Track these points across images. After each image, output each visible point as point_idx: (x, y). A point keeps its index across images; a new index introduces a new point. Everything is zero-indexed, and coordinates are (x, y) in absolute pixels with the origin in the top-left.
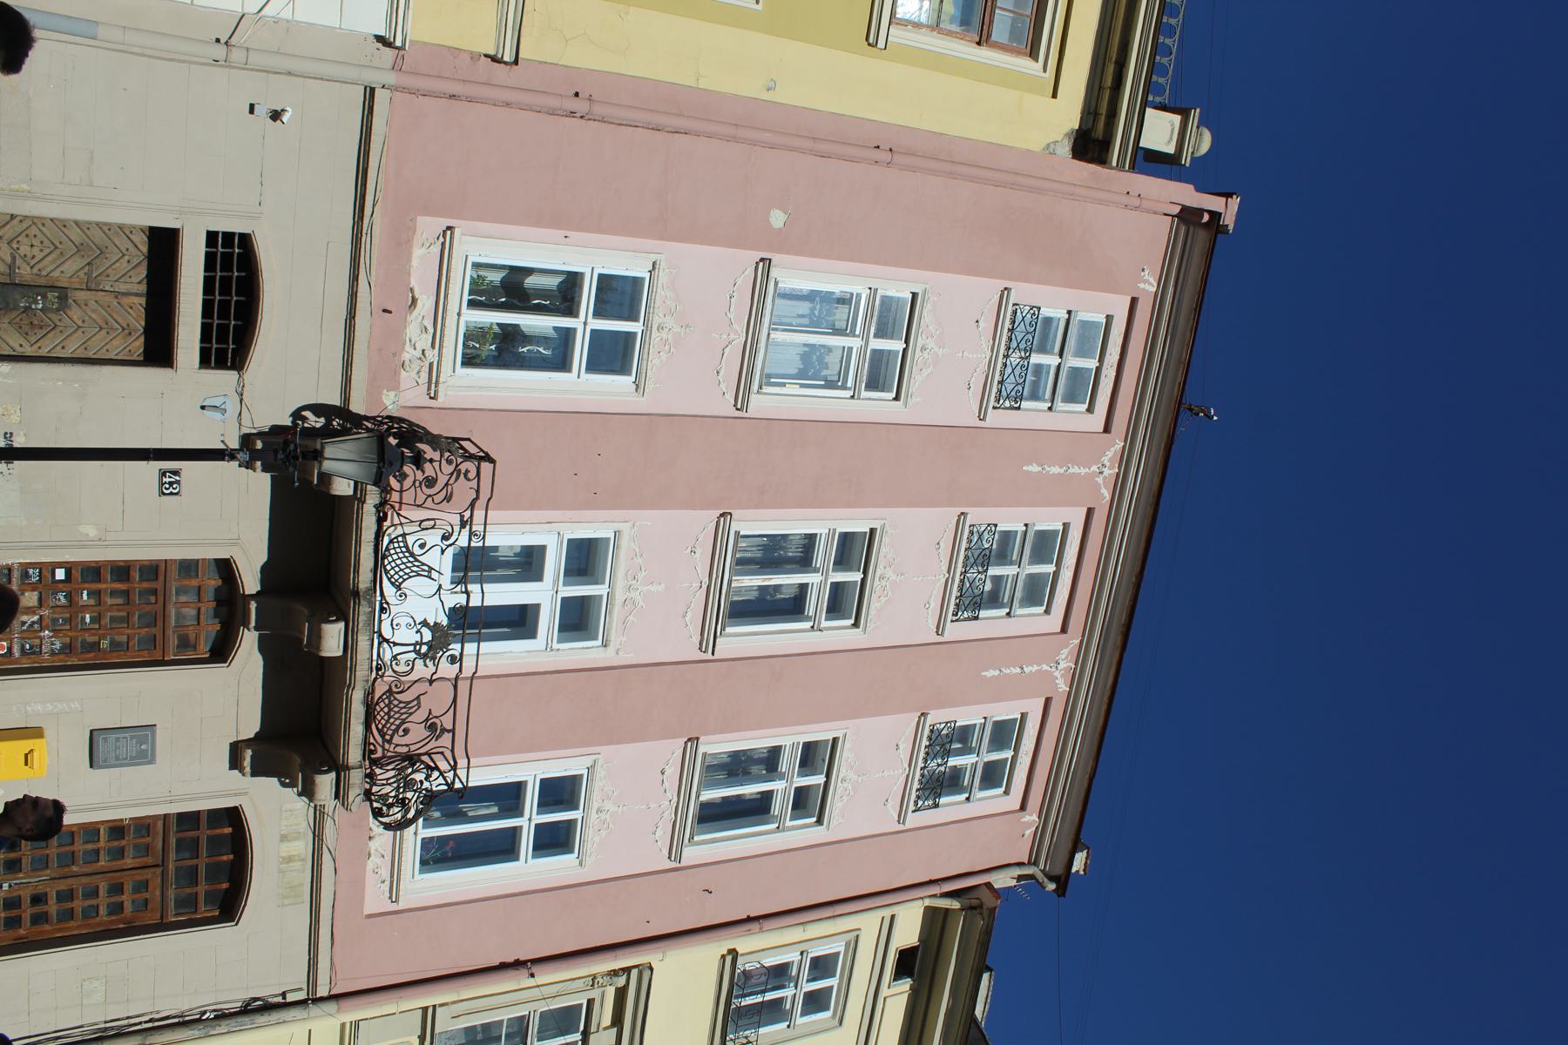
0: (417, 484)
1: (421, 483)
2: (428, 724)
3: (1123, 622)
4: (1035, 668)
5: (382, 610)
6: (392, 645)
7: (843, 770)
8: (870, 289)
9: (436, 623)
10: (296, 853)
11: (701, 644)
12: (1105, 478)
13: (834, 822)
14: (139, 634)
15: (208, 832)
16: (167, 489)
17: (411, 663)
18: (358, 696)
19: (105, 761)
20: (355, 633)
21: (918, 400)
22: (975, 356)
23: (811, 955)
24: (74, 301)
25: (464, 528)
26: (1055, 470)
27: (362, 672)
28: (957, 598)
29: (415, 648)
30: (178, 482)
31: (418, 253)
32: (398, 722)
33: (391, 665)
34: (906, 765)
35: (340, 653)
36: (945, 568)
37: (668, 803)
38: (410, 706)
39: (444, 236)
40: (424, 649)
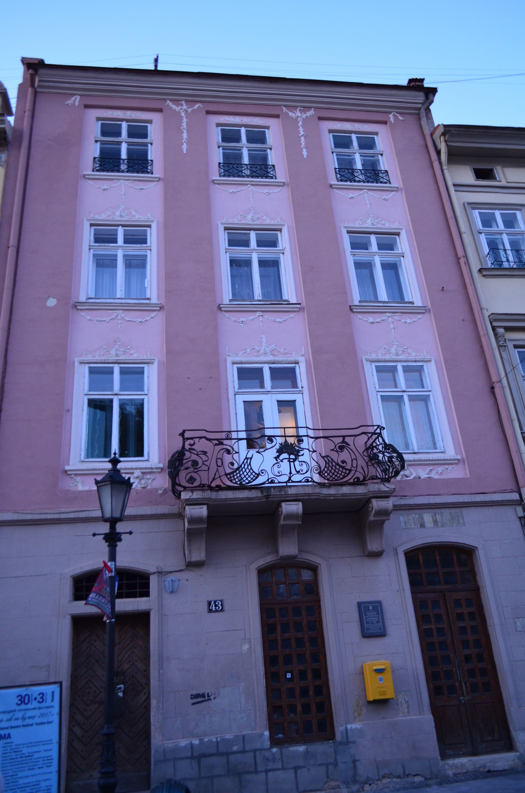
0: (196, 470)
1: (195, 469)
2: (340, 450)
4: (301, 129)
5: (272, 482)
6: (291, 475)
10: (431, 518)
11: (295, 311)
12: (188, 108)
15: (422, 568)
16: (219, 608)
17: (301, 463)
18: (325, 491)
20: (287, 495)
22: (123, 188)
23: (481, 228)
24: (119, 668)
25: (223, 443)
26: (185, 135)
27: (309, 491)
29: (292, 462)
30: (215, 602)
31: (80, 488)
32: (338, 467)
33: (303, 474)
34: (362, 192)
35: (300, 504)
36: (245, 187)
37: (390, 319)
38: (327, 461)
39: (71, 475)
40: (292, 457)
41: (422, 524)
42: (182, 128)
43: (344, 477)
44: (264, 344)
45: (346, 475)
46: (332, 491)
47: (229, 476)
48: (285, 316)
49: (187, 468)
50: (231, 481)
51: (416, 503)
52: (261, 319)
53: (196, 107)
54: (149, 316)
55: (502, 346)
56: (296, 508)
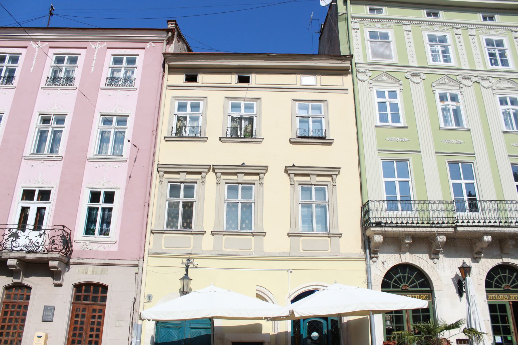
3: (81, 30)
4: (95, 55)
5: (4, 250)
7: (112, 111)
9: (8, 236)
12: (41, 45)
14: (23, 309)
18: (29, 255)
19: (50, 318)
26: (34, 62)
28: (67, 85)
32: (33, 245)
34: (117, 91)
52: (42, 164)
53: (44, 45)
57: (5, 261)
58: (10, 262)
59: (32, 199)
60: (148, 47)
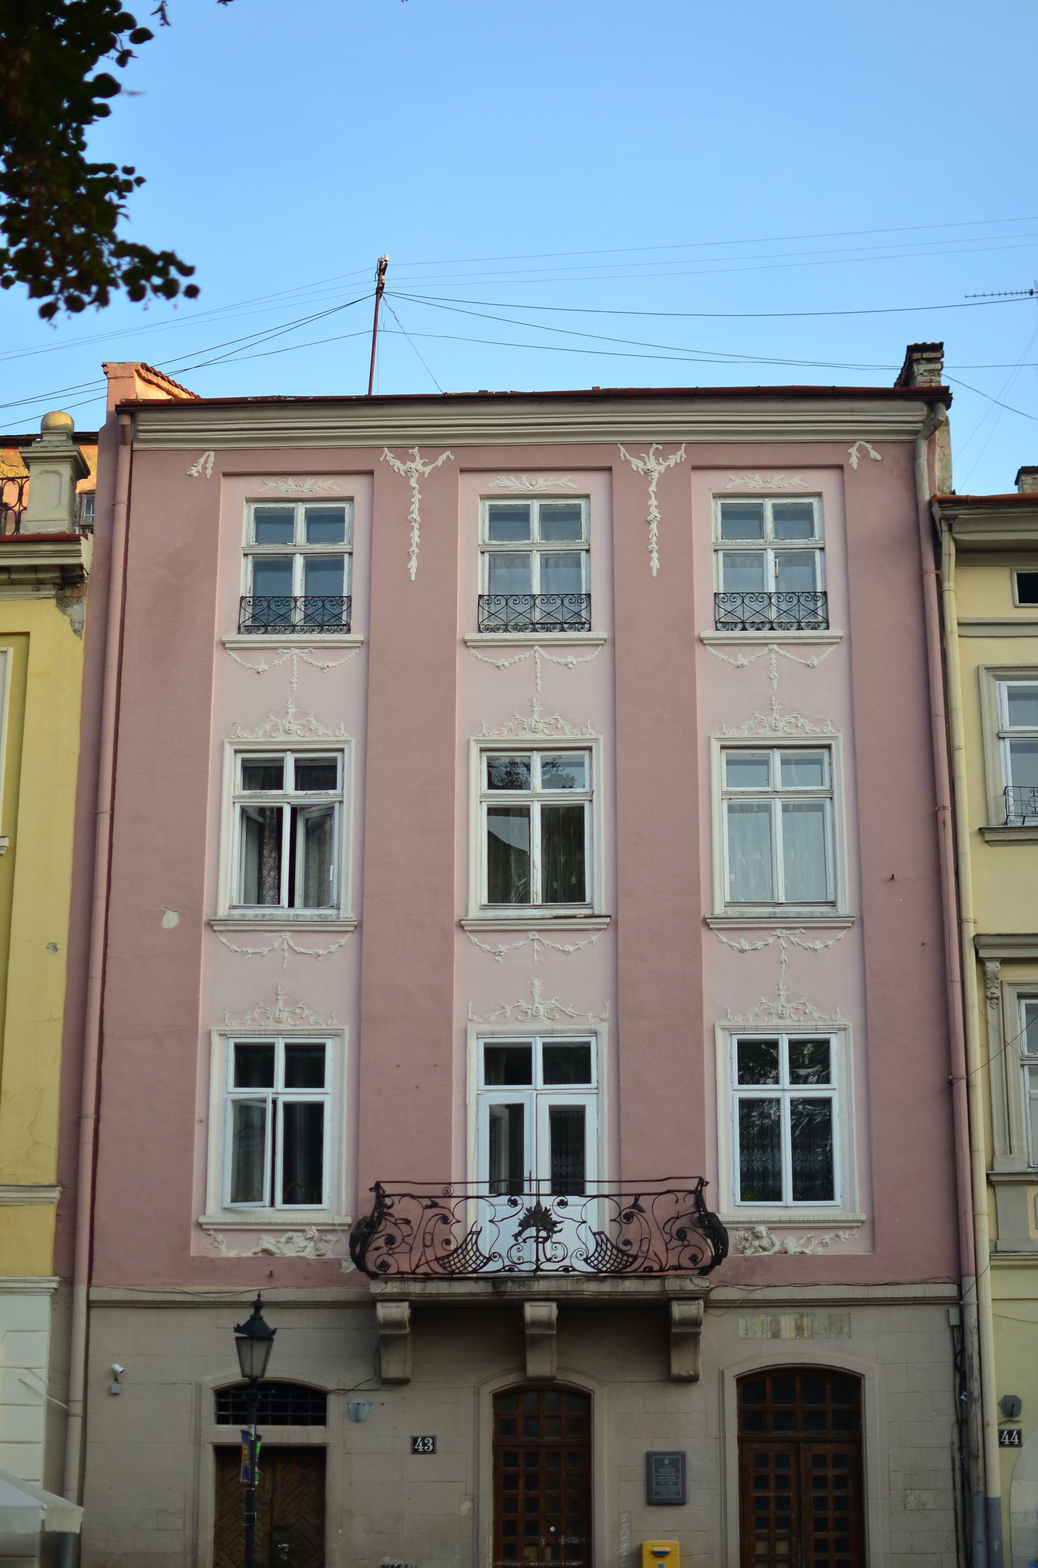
1: (390, 1249)
2: (625, 1221)
4: (653, 502)
5: (511, 1270)
6: (539, 1263)
8: (234, 803)
9: (520, 1225)
10: (793, 1323)
11: (600, 930)
12: (425, 464)
13: (829, 730)
16: (429, 1448)
17: (555, 1245)
19: (678, 1493)
20: (532, 1293)
21: (342, 727)
22: (295, 667)
26: (415, 536)
27: (567, 1286)
28: (563, 630)
29: (541, 1242)
30: (423, 1439)
34: (766, 650)
35: (554, 1305)
36: (527, 653)
37: (782, 941)
39: (208, 1230)
40: (543, 1234)
41: (775, 1333)
42: (410, 517)
43: (626, 1267)
44: (537, 999)
45: (628, 1264)
46: (607, 1287)
47: (441, 1262)
48: (583, 941)
49: (377, 1249)
50: (445, 1268)
51: (768, 1298)
53: (439, 462)
54: (335, 943)
55: (991, 999)
56: (547, 1311)
57: (516, 1308)
58: (533, 1311)
59: (525, 1078)
60: (854, 461)
